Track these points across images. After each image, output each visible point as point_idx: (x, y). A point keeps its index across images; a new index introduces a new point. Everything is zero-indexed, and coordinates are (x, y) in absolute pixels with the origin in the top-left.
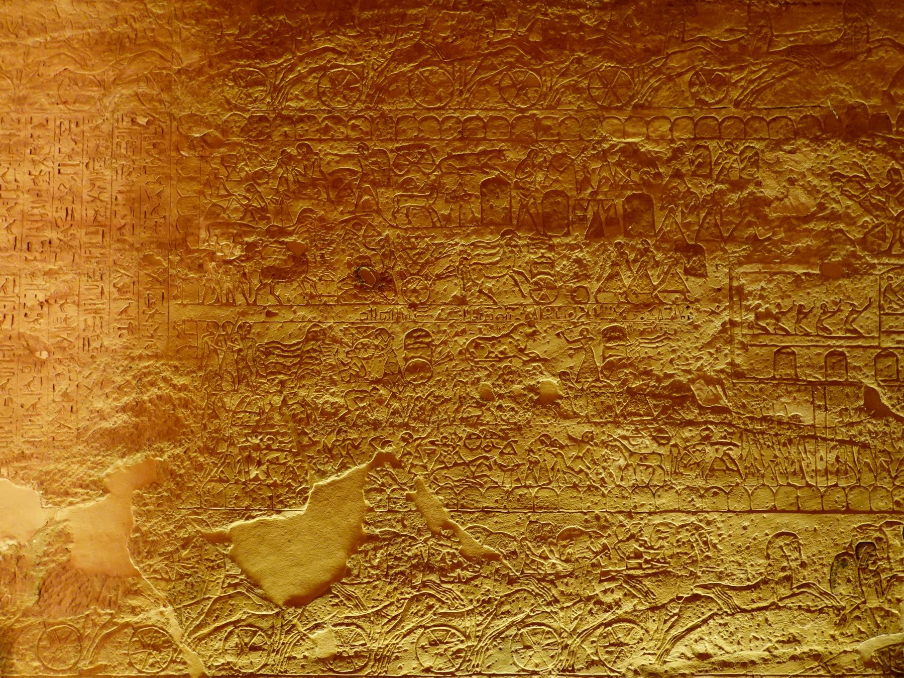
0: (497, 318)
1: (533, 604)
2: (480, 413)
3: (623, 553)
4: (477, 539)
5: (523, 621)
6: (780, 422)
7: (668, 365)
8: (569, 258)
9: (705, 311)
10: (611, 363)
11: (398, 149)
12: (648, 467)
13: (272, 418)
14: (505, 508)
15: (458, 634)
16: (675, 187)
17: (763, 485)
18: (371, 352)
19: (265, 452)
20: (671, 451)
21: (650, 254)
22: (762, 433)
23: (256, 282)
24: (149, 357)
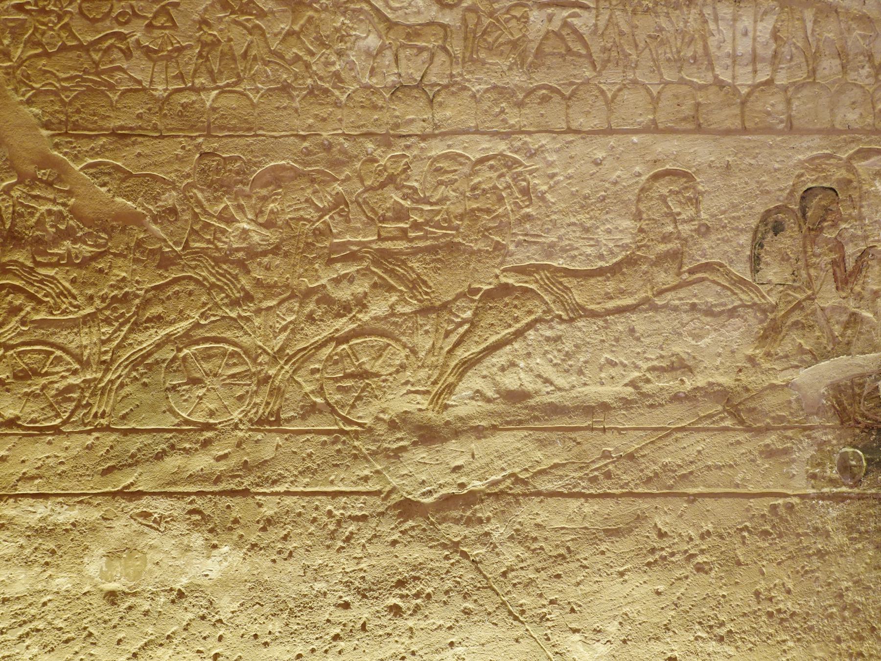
1: (204, 304)
4: (104, 185)
5: (187, 334)
12: (421, 50)
14: (155, 128)
15: (68, 358)
17: (635, 82)
20: (464, 20)
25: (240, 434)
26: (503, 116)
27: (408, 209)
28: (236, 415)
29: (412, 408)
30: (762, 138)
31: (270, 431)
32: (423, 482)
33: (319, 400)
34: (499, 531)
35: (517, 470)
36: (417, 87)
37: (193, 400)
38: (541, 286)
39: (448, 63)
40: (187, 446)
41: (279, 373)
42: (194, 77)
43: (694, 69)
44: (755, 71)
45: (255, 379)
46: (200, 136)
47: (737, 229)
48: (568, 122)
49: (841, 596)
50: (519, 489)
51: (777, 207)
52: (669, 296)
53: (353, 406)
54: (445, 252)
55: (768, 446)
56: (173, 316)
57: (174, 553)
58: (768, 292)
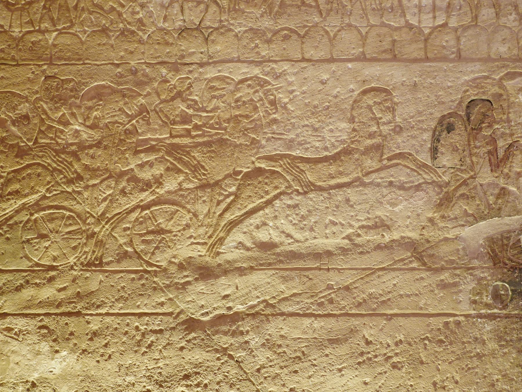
1: (49, 183)
3: (166, 116)
5: (37, 203)
14: (13, 59)
17: (350, 25)
25: (75, 273)
26: (257, 50)
27: (191, 116)
28: (72, 260)
29: (195, 254)
30: (439, 64)
31: (95, 271)
32: (203, 306)
33: (129, 249)
34: (255, 340)
35: (267, 298)
36: (196, 29)
37: (41, 249)
38: (284, 169)
39: (218, 12)
40: (38, 281)
41: (101, 230)
42: (40, 22)
43: (391, 16)
44: (434, 17)
45: (84, 235)
46: (45, 64)
47: (421, 129)
48: (303, 53)
49: (493, 385)
50: (268, 311)
51: (449, 114)
52: (374, 176)
53: (153, 253)
54: (217, 145)
55: (442, 280)
56: (27, 191)
57: (29, 356)
58: (443, 173)
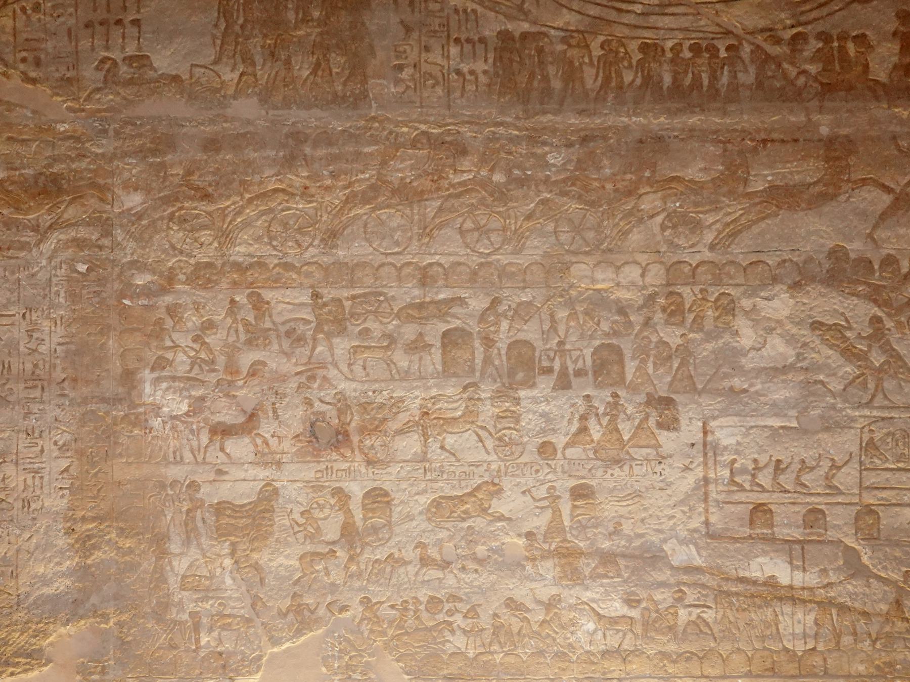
0: (460, 476)
2: (442, 576)
6: (755, 583)
7: (639, 523)
8: (535, 413)
9: (679, 468)
10: (579, 521)
11: (354, 297)
12: (618, 631)
13: (224, 582)
14: (469, 675)
16: (647, 337)
17: (738, 649)
18: (327, 511)
19: (216, 618)
20: (642, 615)
21: (620, 407)
22: (737, 594)
23: (205, 439)
24: (94, 519)
42: (490, 645)
